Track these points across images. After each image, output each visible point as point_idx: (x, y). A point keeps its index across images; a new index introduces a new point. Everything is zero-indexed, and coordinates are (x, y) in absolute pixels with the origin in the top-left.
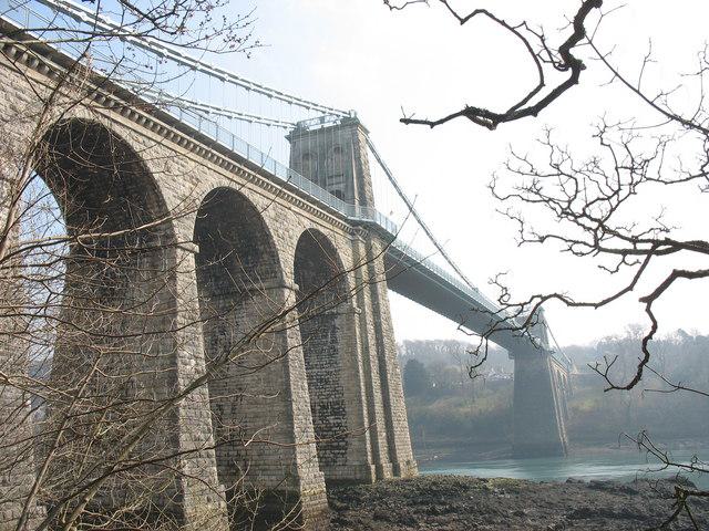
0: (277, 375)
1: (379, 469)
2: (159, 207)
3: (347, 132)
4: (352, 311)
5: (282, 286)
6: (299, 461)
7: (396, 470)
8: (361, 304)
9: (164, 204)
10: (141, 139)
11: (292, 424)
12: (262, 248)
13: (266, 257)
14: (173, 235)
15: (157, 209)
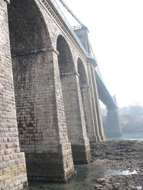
0: (75, 105)
1: (98, 138)
2: (46, 35)
3: (83, 31)
4: (88, 87)
5: (75, 74)
6: (84, 135)
7: (102, 139)
8: (91, 85)
9: (49, 34)
10: (42, 7)
11: (81, 121)
12: (68, 61)
13: (69, 64)
14: (51, 46)
15: (45, 36)
